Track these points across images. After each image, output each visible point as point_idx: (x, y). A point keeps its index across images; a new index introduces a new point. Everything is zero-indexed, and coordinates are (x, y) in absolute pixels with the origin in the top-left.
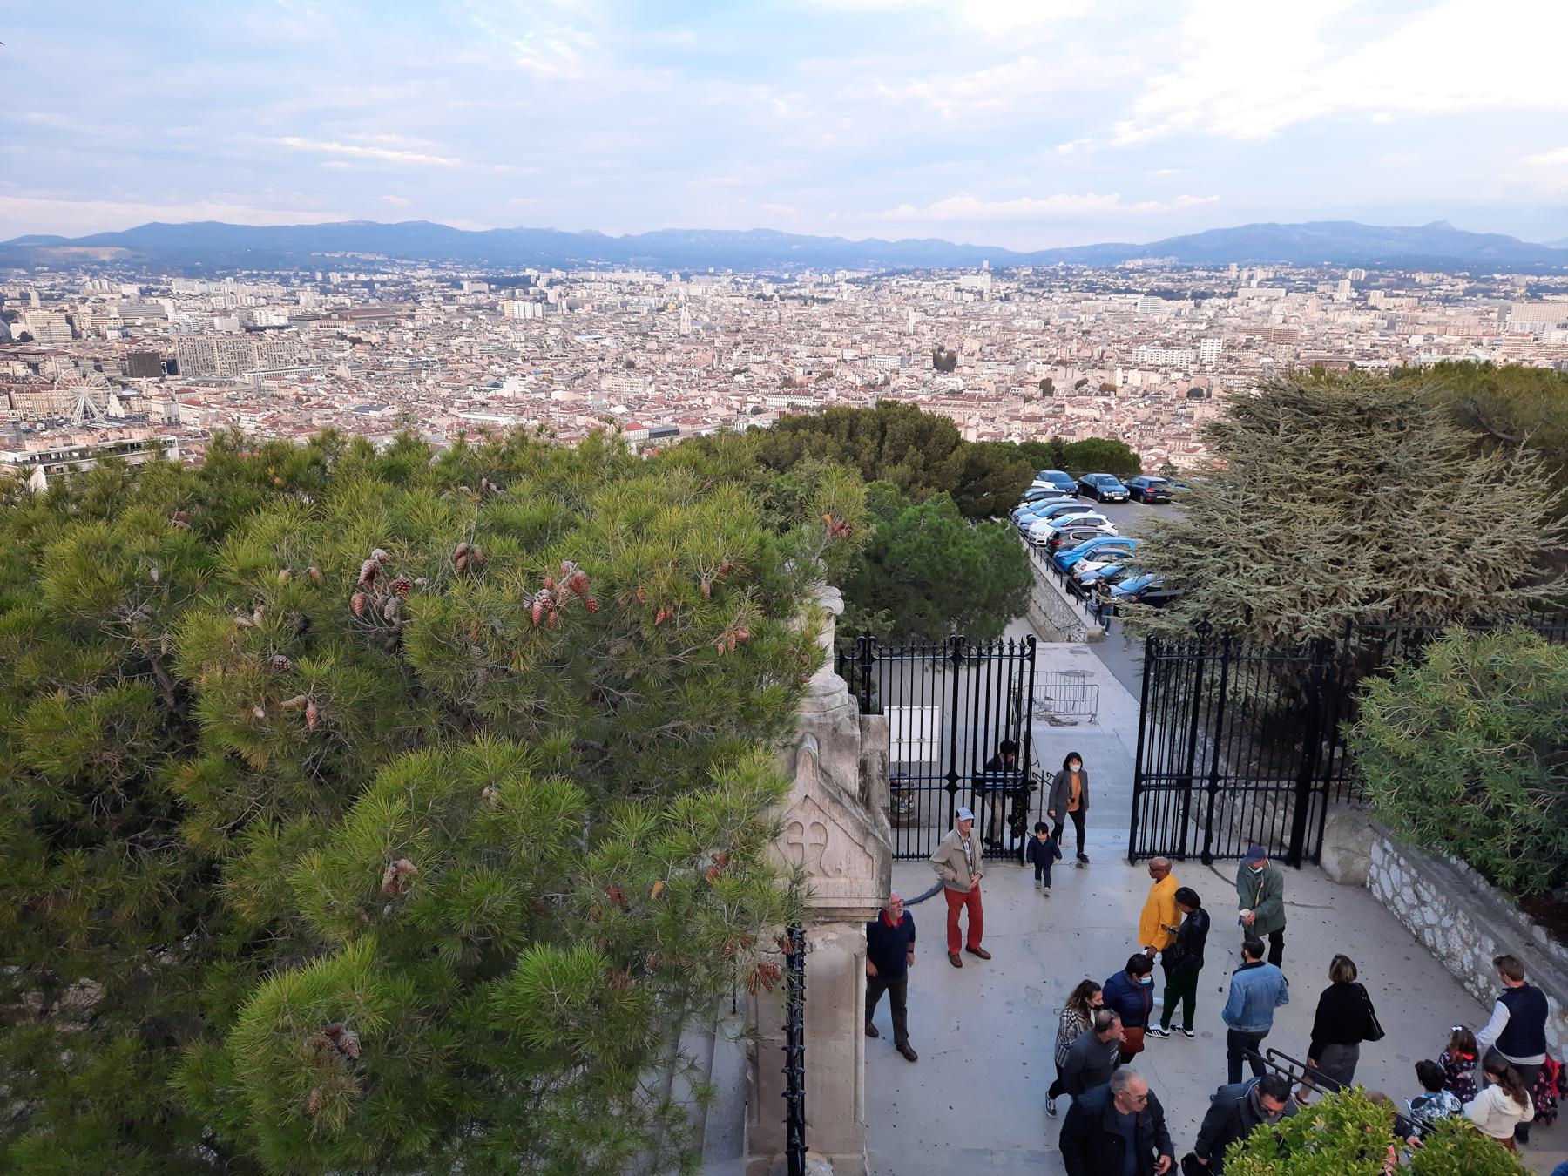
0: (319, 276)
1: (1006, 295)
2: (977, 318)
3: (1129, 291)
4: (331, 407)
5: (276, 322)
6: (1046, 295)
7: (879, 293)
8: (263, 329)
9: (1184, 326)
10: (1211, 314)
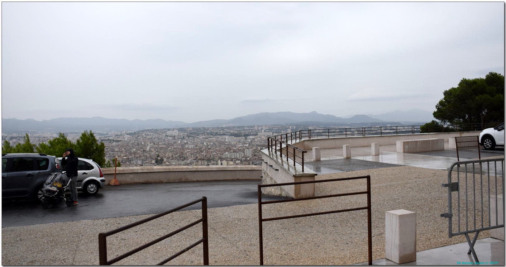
1: (183, 137)
2: (172, 145)
3: (224, 134)
6: (196, 137)
7: (138, 138)
9: (241, 145)
10: (250, 141)
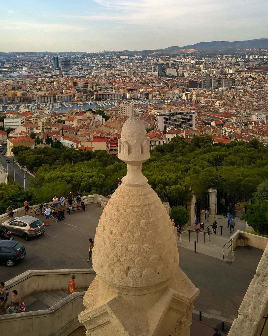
0: (247, 57)
4: (243, 100)
5: (231, 72)
8: (227, 74)
